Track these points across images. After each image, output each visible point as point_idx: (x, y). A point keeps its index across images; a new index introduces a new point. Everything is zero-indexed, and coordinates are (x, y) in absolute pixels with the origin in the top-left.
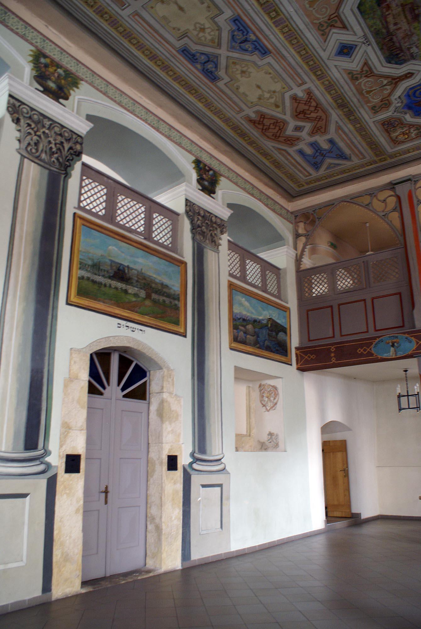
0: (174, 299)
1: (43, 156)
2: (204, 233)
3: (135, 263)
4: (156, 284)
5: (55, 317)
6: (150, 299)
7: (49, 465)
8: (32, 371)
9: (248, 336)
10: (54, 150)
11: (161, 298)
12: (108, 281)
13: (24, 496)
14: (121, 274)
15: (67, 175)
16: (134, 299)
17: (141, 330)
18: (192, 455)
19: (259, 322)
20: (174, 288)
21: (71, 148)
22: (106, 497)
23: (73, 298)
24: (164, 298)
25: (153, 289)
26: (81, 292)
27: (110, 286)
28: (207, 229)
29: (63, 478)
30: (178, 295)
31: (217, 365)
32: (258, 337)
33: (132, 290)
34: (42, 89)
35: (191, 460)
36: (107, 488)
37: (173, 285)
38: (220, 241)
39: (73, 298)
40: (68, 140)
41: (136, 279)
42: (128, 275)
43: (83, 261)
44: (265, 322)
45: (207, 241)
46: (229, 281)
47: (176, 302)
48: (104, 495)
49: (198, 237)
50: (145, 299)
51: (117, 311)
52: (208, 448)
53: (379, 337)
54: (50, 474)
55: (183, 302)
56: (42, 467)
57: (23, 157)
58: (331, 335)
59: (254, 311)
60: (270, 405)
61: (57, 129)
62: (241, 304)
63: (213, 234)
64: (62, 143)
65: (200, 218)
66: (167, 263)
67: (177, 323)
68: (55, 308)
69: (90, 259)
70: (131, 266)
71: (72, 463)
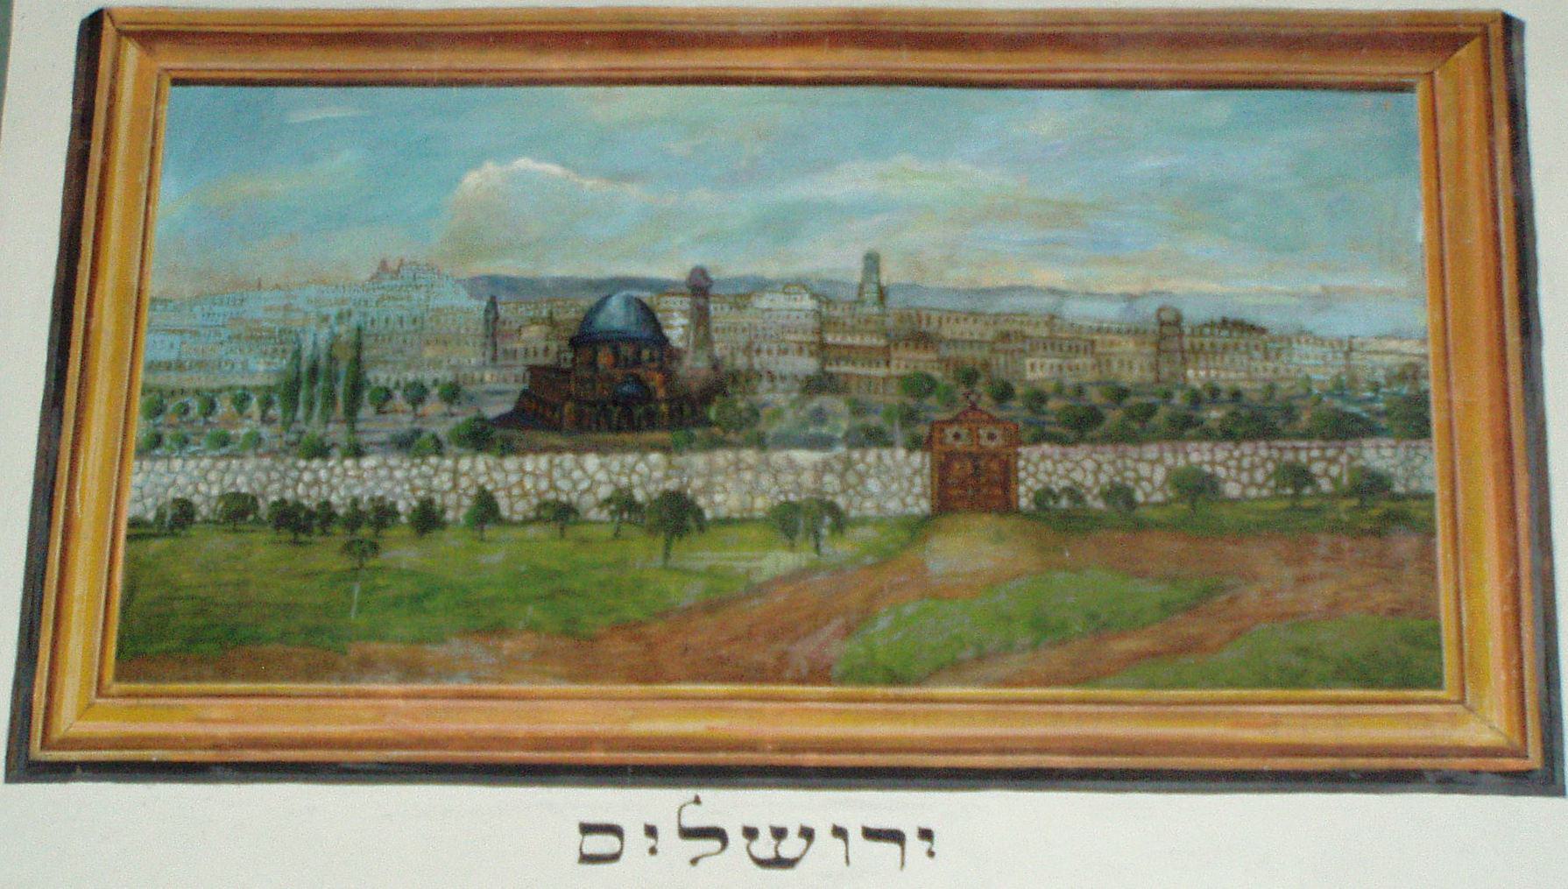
0: (1344, 428)
3: (783, 225)
6: (1007, 507)
11: (1151, 470)
12: (457, 477)
14: (612, 375)
16: (780, 560)
17: (896, 836)
20: (1339, 324)
24: (1199, 455)
25: (1038, 398)
26: (158, 640)
27: (486, 509)
30: (1411, 373)
33: (727, 481)
37: (1324, 301)
39: (76, 716)
41: (807, 365)
42: (693, 367)
43: (172, 380)
47: (1379, 455)
50: (918, 528)
66: (1220, 105)
69: (254, 337)
70: (730, 266)
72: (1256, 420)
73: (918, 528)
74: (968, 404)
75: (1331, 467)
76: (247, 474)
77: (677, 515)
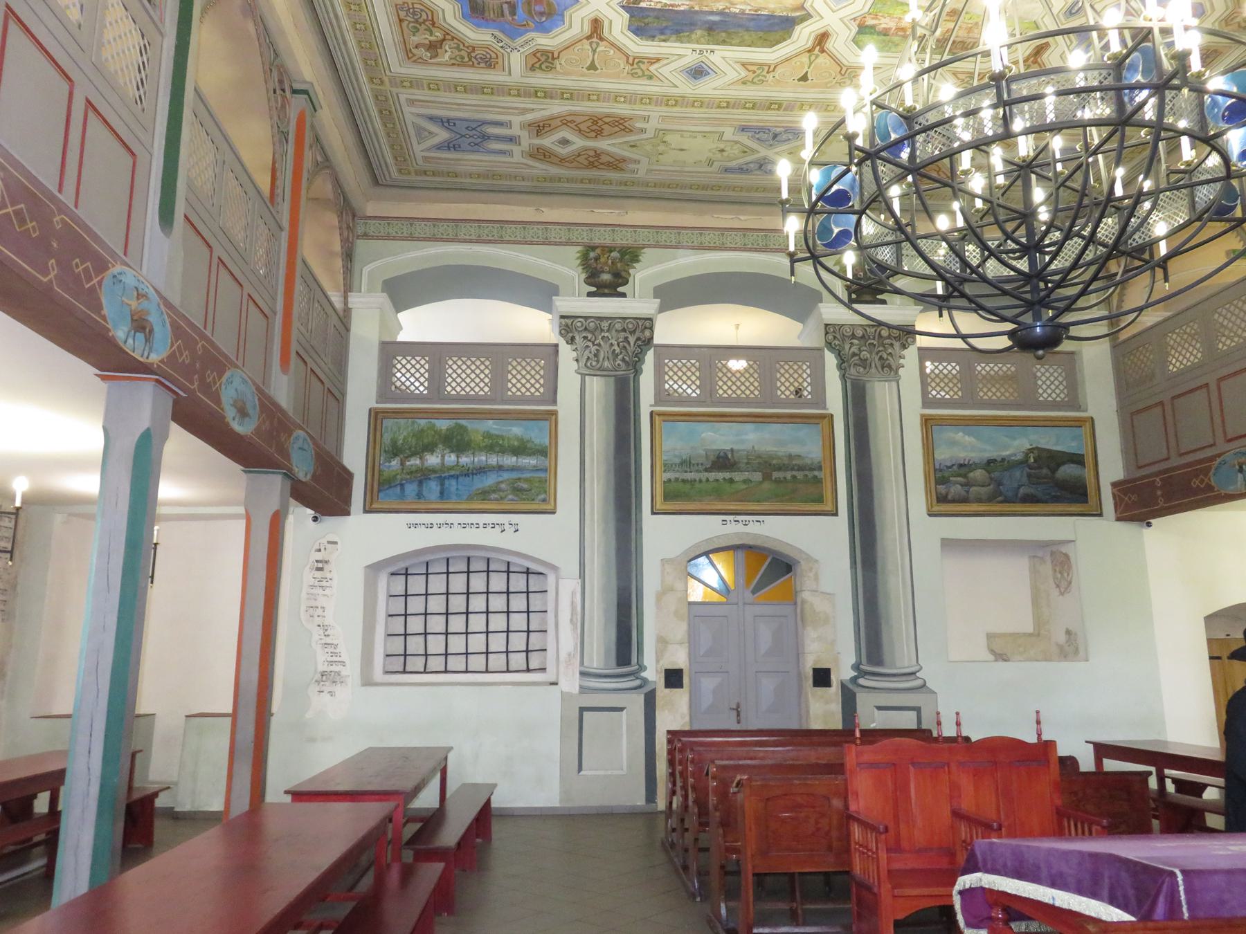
0: (812, 469)
1: (606, 364)
2: (866, 360)
4: (779, 458)
5: (639, 531)
7: (645, 681)
8: (619, 589)
9: (973, 489)
10: (618, 350)
11: (789, 475)
13: (621, 709)
14: (723, 462)
15: (638, 372)
16: (744, 486)
18: (856, 667)
19: (1003, 460)
20: (813, 455)
21: (638, 339)
22: (738, 715)
23: (659, 505)
24: (794, 473)
26: (668, 497)
27: (707, 480)
28: (871, 353)
29: (663, 693)
31: (901, 543)
32: (1000, 484)
33: (737, 476)
34: (594, 289)
35: (854, 674)
36: (738, 706)
38: (902, 361)
39: (659, 506)
40: (633, 332)
44: (1019, 457)
45: (873, 370)
46: (922, 416)
47: (816, 473)
48: (735, 713)
49: (853, 371)
50: (761, 483)
51: (720, 506)
52: (887, 657)
53: (1219, 455)
54: (647, 689)
55: (828, 471)
56: (638, 682)
57: (583, 375)
58: (1165, 455)
59: (988, 447)
60: (1064, 584)
61: (618, 326)
62: (953, 443)
63: (885, 356)
64: (626, 338)
65: (855, 341)
67: (820, 499)
68: (639, 521)
70: (735, 448)
71: (673, 678)
72: (801, 468)
73: (761, 483)
74: (768, 466)
75: (810, 474)
76: (677, 475)
77: (731, 481)
